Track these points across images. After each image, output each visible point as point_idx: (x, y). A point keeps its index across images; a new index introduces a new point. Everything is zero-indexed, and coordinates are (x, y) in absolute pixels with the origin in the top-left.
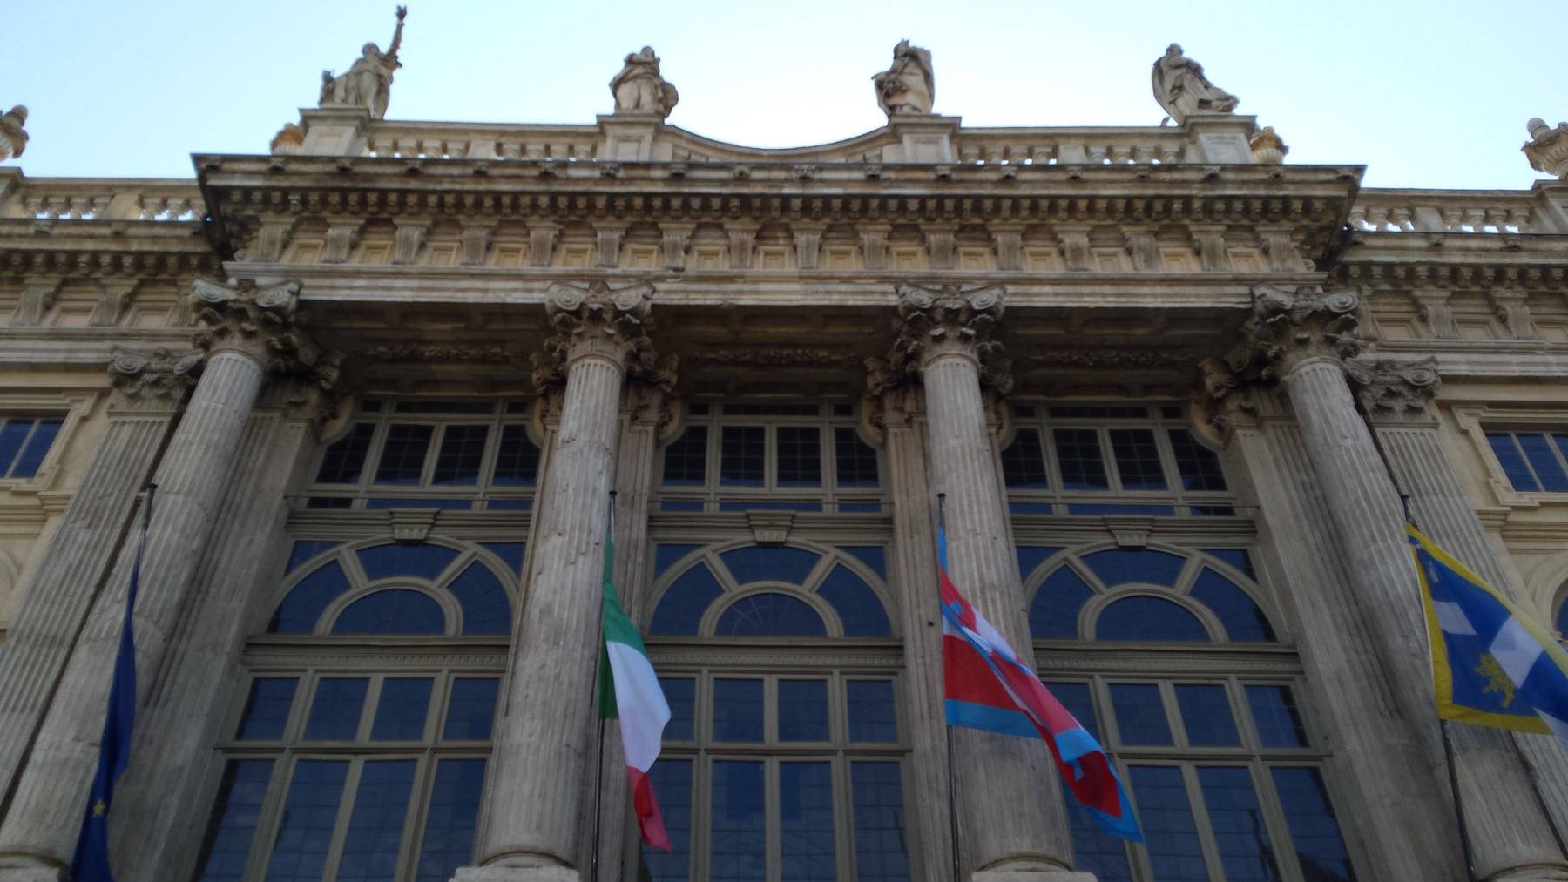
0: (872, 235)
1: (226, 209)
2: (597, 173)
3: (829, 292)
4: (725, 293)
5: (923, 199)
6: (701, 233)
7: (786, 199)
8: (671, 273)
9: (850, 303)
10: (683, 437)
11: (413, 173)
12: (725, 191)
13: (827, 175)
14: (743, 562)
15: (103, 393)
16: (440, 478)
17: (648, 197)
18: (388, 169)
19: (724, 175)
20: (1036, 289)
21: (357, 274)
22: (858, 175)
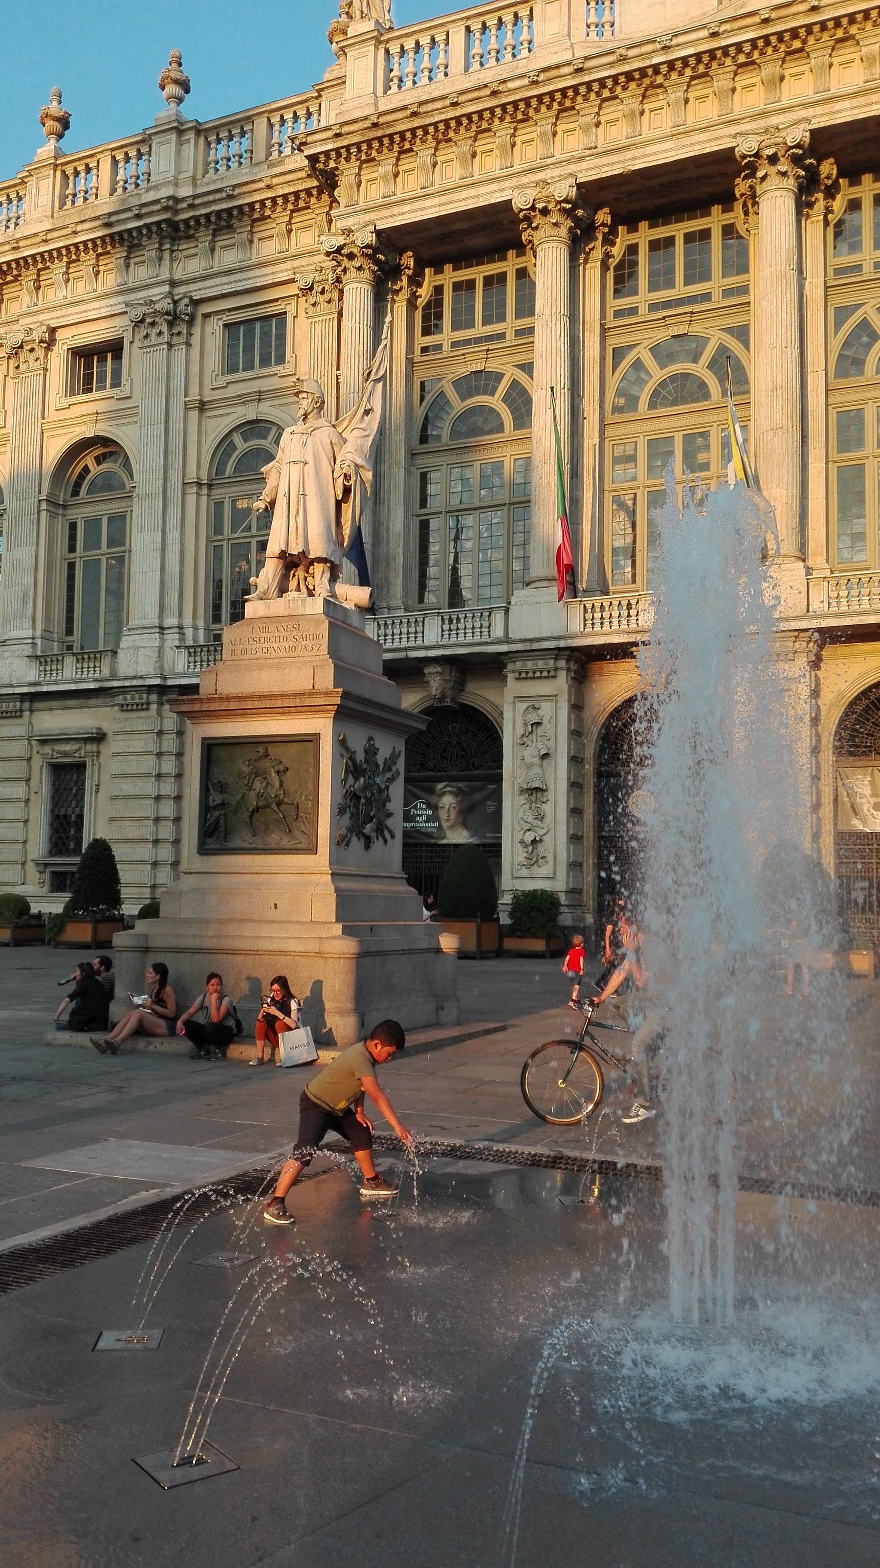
0: (722, 79)
1: (320, 166)
2: (526, 81)
3: (692, 144)
4: (624, 161)
5: (753, 42)
6: (605, 104)
7: (656, 69)
8: (588, 152)
9: (708, 150)
10: (624, 256)
11: (415, 114)
12: (613, 72)
13: (681, 39)
14: (661, 353)
15: (297, 295)
16: (484, 324)
17: (563, 91)
18: (400, 115)
19: (610, 58)
20: (839, 106)
21: (403, 201)
22: (704, 33)
